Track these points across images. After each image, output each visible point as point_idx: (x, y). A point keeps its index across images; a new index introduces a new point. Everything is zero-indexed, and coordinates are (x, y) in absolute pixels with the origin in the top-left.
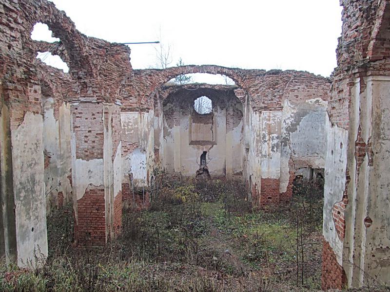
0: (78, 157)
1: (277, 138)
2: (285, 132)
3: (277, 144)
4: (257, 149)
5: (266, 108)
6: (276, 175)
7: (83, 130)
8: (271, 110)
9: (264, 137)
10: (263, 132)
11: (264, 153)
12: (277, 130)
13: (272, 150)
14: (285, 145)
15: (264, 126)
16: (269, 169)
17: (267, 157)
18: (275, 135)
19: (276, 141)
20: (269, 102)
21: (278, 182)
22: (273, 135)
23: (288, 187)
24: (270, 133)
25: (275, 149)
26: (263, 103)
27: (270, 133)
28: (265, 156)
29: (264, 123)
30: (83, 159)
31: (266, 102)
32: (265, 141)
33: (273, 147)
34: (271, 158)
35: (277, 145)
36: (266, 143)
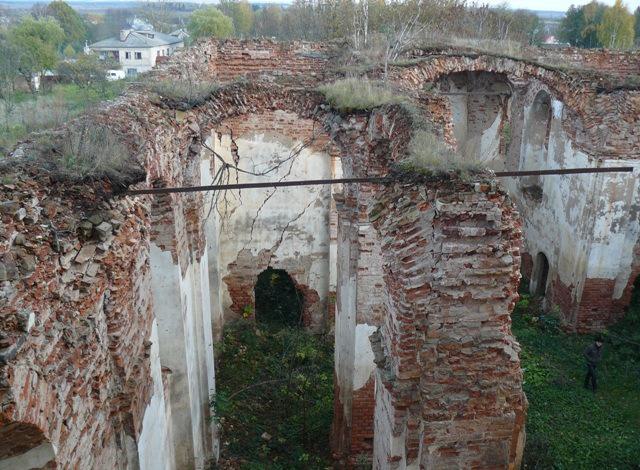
0: (359, 321)
1: (624, 208)
2: (637, 195)
3: (622, 219)
4: (585, 226)
5: (612, 155)
6: (611, 272)
7: (373, 273)
8: (620, 158)
9: (602, 205)
10: (602, 198)
11: (596, 235)
12: (625, 194)
13: (612, 230)
14: (633, 219)
15: (604, 187)
16: (600, 262)
17: (602, 241)
18: (621, 203)
19: (620, 214)
20: (620, 142)
21: (610, 285)
22: (617, 203)
23: (625, 291)
24: (612, 200)
25: (617, 228)
26: (609, 144)
27: (612, 200)
28: (598, 240)
29: (605, 181)
30: (369, 324)
31: (614, 143)
32: (602, 214)
33: (614, 225)
34: (608, 244)
35: (622, 221)
36: (603, 218)
